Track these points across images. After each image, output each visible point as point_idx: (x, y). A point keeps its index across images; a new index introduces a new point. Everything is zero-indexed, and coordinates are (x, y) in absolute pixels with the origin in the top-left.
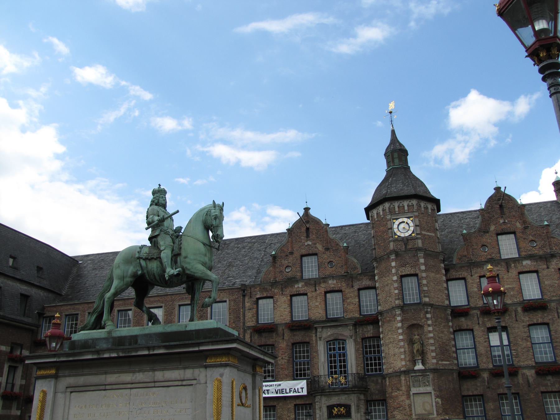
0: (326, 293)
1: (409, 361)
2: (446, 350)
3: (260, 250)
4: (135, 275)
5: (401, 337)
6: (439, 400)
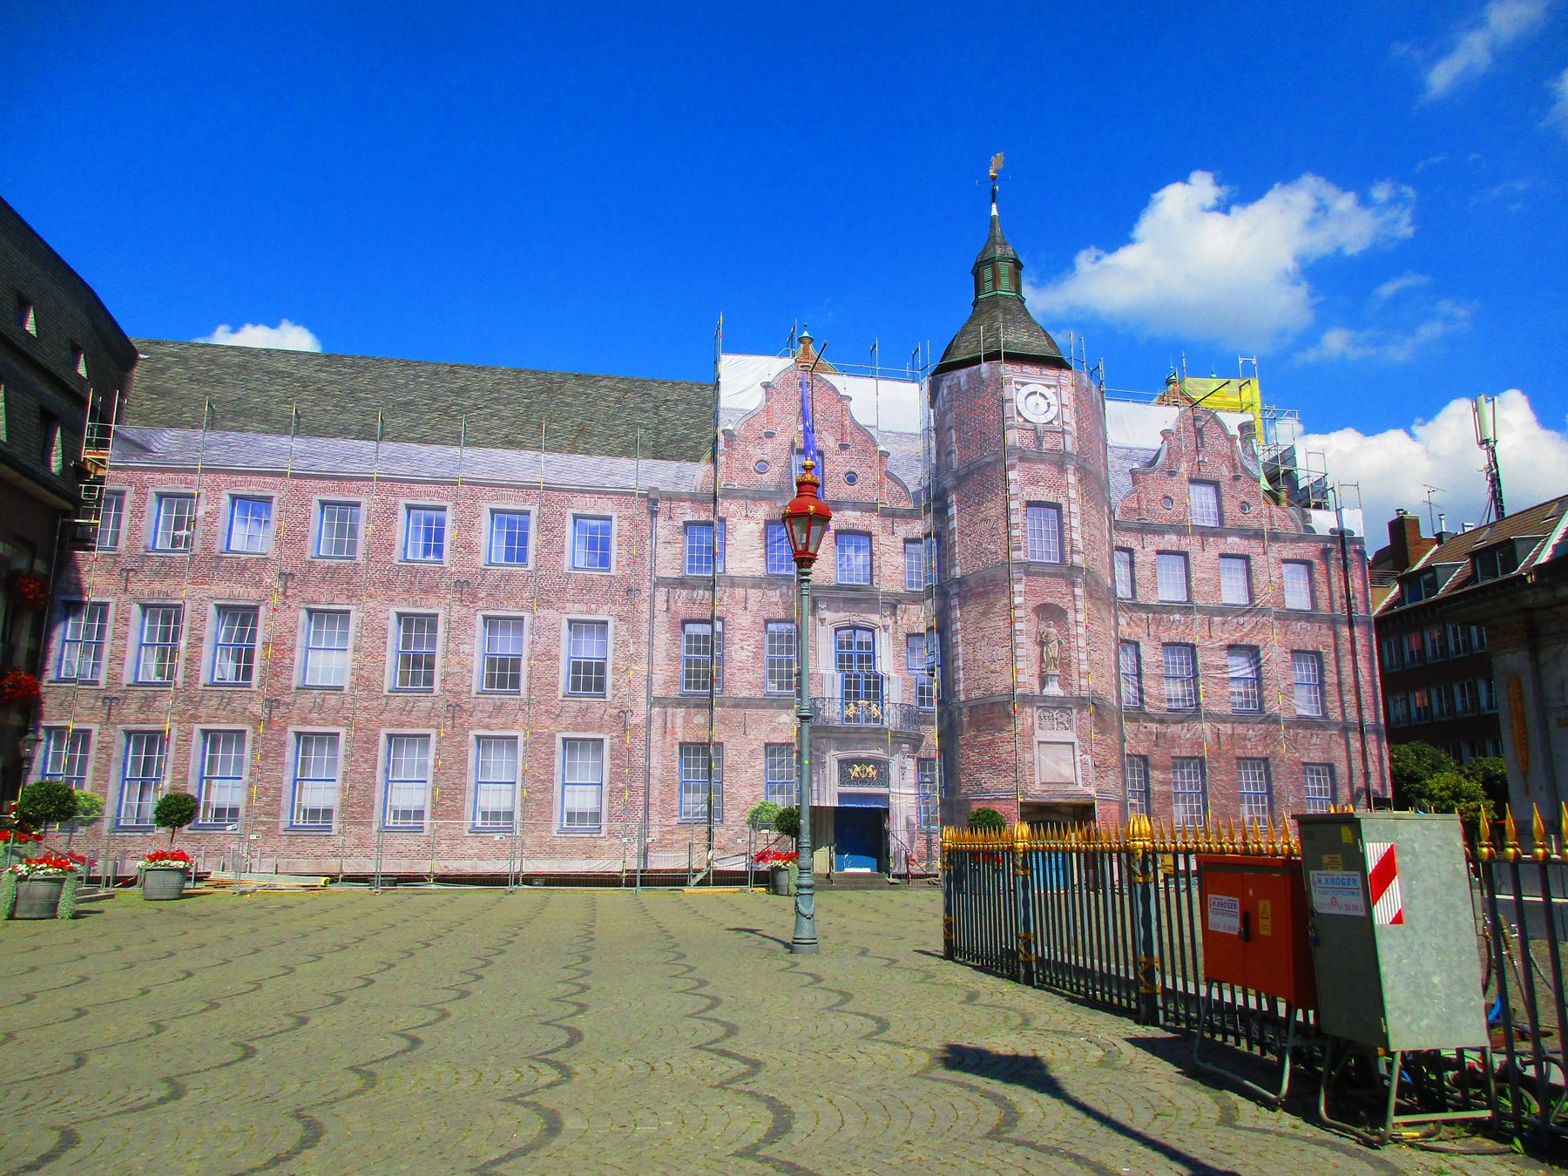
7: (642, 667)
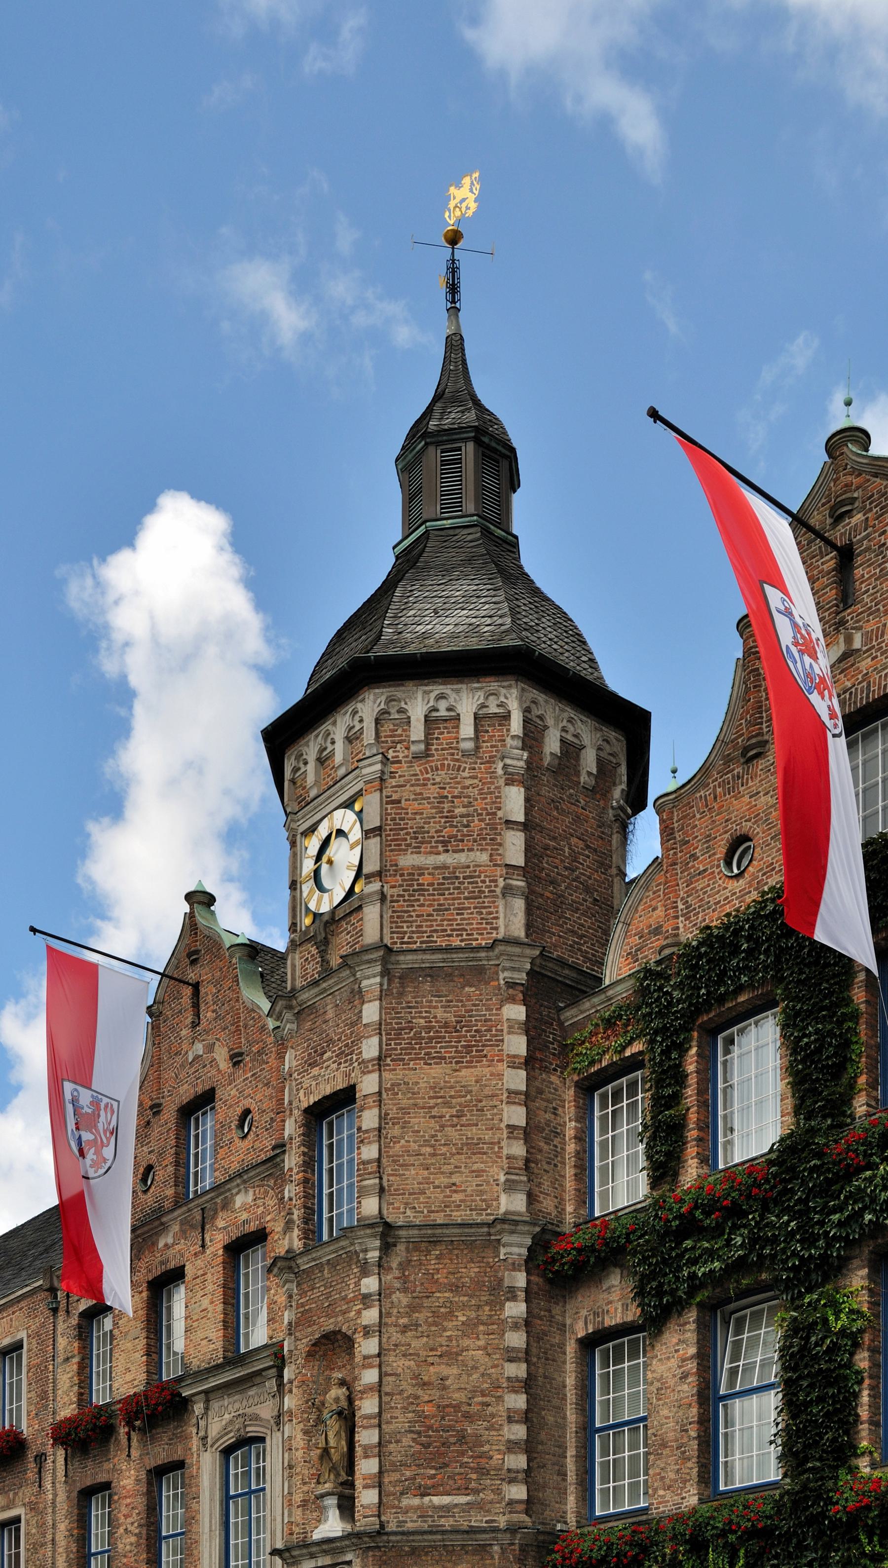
2: (462, 1438)
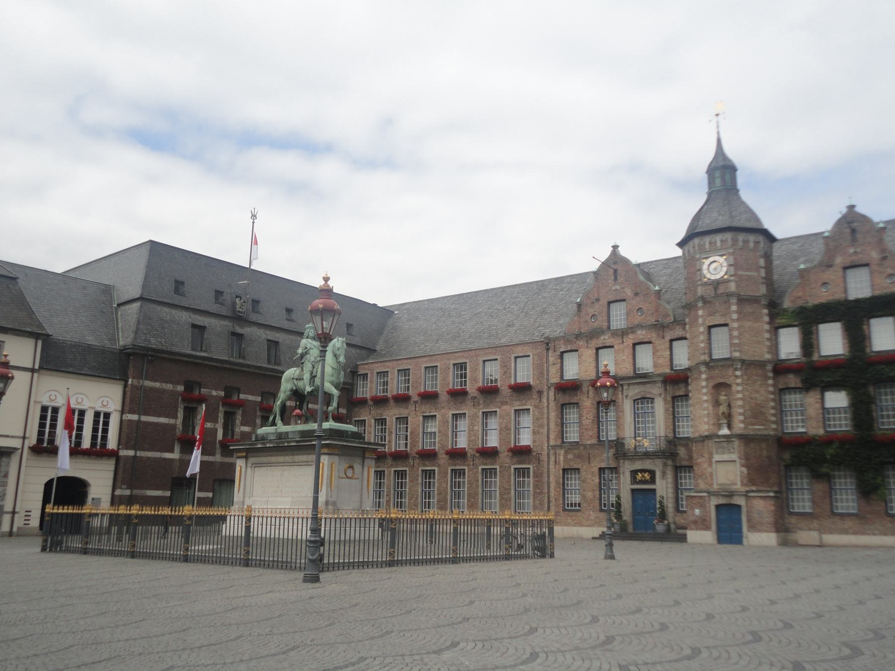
0: (634, 345)
1: (713, 424)
2: (761, 412)
3: (578, 293)
4: (292, 390)
5: (705, 398)
6: (745, 470)
7: (545, 430)
